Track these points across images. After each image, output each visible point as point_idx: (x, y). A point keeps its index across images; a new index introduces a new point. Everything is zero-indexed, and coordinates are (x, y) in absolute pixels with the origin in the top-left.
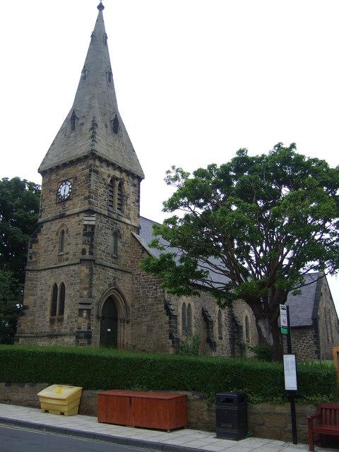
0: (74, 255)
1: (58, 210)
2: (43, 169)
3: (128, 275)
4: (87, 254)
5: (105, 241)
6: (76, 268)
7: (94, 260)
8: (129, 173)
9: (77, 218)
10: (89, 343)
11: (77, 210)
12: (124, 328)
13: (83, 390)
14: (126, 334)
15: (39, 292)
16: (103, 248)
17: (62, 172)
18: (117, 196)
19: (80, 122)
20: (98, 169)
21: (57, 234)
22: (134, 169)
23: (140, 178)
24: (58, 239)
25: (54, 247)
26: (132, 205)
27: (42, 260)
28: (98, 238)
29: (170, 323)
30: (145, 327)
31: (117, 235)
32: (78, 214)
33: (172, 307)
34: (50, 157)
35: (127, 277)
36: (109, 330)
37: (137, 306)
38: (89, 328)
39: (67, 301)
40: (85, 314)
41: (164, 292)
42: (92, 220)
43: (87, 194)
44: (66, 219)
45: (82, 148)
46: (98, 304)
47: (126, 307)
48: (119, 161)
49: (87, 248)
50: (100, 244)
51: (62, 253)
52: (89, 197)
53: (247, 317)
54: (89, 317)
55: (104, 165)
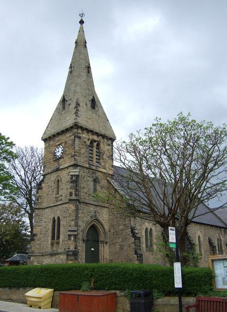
0: (66, 197)
2: (46, 136)
3: (106, 209)
4: (74, 195)
5: (87, 185)
6: (66, 205)
7: (78, 200)
8: (104, 136)
9: (67, 170)
10: (76, 259)
11: (67, 165)
12: (104, 247)
13: (54, 291)
14: (106, 252)
15: (44, 224)
16: (85, 191)
17: (57, 139)
18: (95, 153)
19: (68, 103)
20: (81, 135)
21: (54, 183)
22: (108, 134)
23: (112, 140)
26: (107, 159)
27: (45, 201)
28: (82, 184)
29: (135, 243)
30: (118, 246)
31: (96, 181)
32: (67, 168)
33: (136, 231)
34: (49, 129)
35: (105, 211)
36: (93, 249)
37: (112, 231)
38: (76, 248)
39: (62, 229)
40: (72, 238)
41: (130, 221)
42: (75, 171)
43: (73, 153)
44: (60, 172)
45: (69, 121)
46: (82, 231)
47: (105, 233)
48: (96, 129)
49: (73, 191)
50: (84, 188)
51: (57, 196)
52: (74, 155)
53: (199, 237)
54: (75, 241)
55: (85, 132)
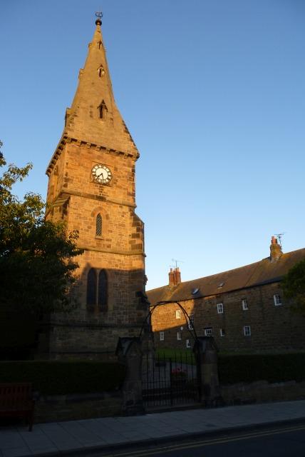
0: (118, 244)
1: (95, 190)
9: (120, 209)
24: (94, 220)
25: (89, 228)
44: (105, 203)
